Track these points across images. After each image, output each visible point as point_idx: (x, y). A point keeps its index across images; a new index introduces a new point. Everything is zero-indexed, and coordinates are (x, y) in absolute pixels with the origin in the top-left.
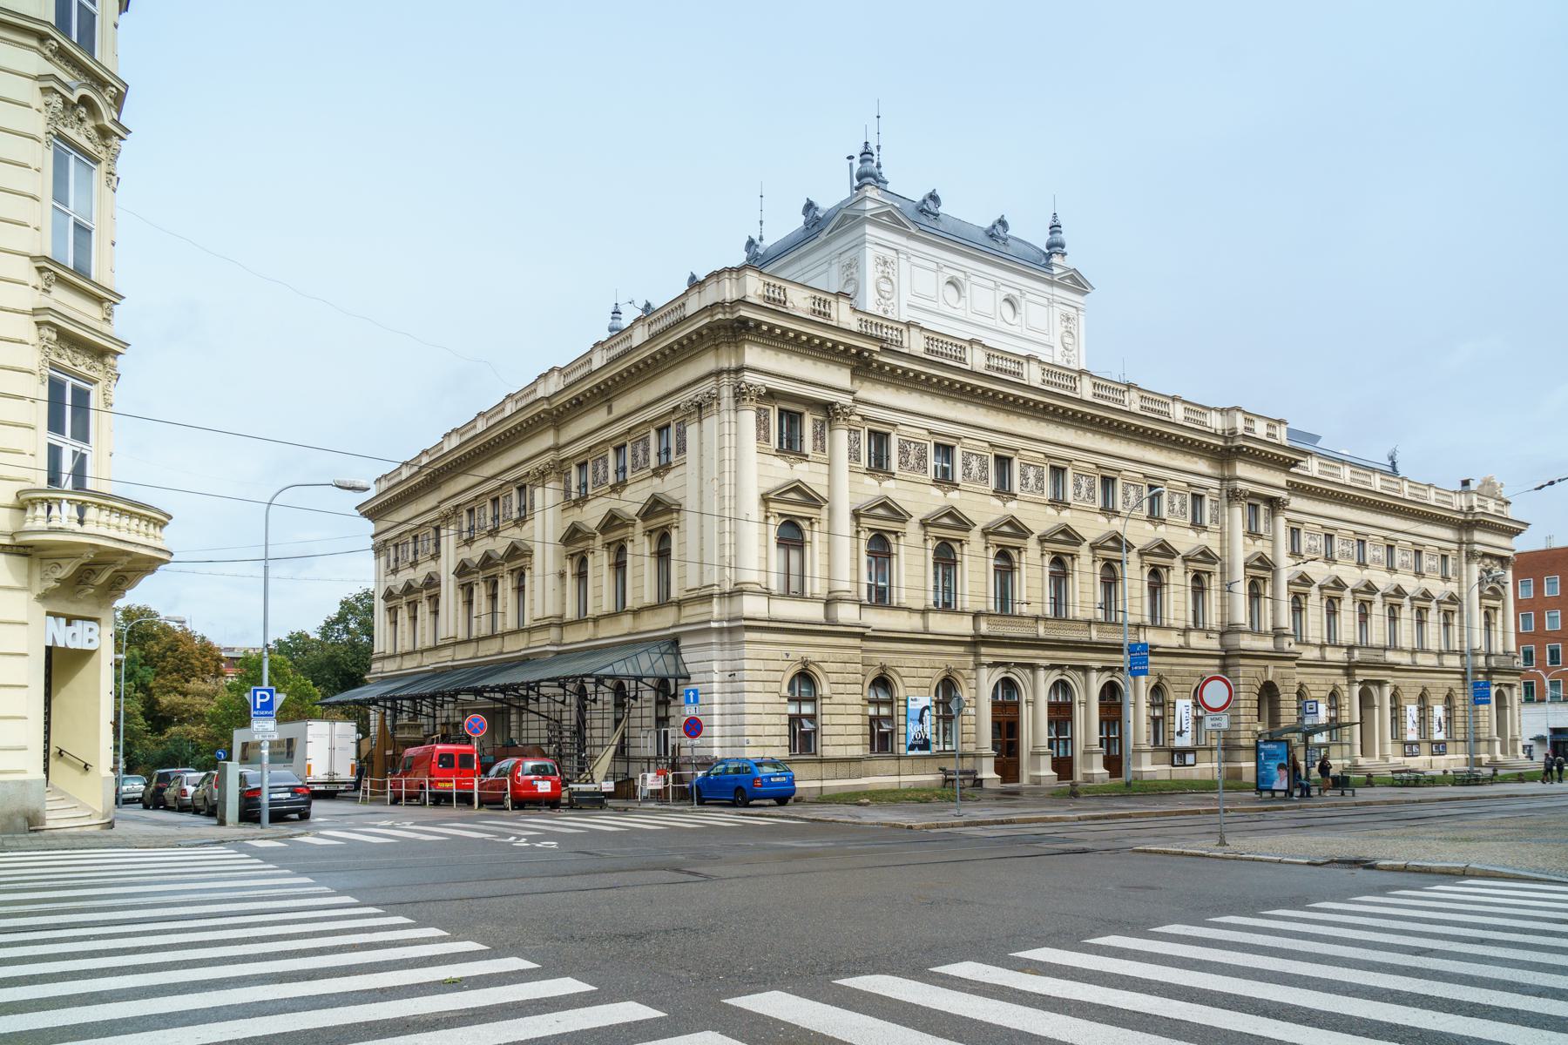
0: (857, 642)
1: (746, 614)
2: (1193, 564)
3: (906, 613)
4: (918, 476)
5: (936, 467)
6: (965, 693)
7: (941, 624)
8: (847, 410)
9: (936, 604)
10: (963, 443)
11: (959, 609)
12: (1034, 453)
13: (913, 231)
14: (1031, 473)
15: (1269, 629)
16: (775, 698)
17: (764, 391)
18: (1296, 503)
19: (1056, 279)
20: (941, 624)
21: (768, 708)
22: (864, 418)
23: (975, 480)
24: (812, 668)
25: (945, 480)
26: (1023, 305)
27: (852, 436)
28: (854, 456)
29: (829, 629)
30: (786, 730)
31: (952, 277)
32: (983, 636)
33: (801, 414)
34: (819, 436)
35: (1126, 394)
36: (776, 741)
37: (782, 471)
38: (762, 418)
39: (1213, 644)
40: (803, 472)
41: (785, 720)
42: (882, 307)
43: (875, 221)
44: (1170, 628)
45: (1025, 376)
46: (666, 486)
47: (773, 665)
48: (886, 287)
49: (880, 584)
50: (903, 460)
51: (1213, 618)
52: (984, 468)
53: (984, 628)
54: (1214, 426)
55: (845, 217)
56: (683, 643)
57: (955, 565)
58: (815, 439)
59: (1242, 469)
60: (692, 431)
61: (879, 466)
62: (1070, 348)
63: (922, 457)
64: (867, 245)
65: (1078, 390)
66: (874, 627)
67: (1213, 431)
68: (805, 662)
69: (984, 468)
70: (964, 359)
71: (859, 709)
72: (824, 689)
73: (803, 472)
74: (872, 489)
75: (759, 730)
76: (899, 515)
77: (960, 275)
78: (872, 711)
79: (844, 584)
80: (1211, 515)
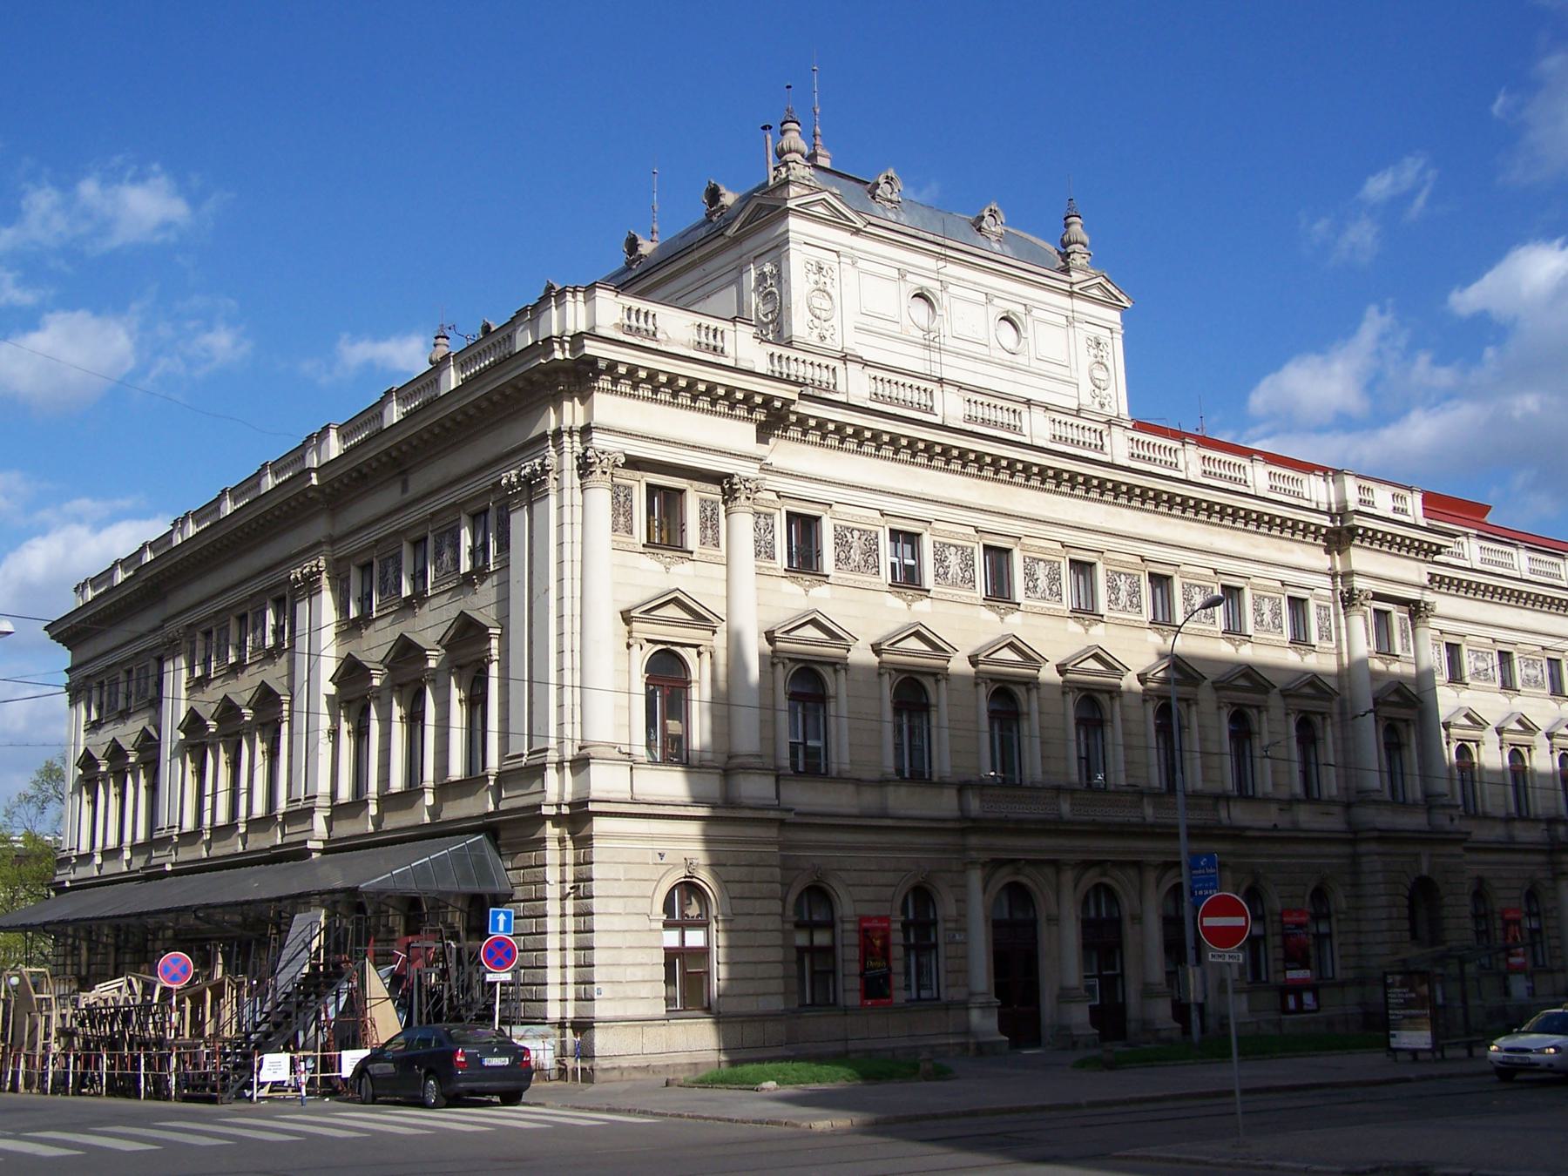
0: (772, 833)
1: (594, 795)
2: (1296, 701)
3: (851, 788)
4: (867, 579)
5: (893, 565)
6: (946, 907)
7: (905, 801)
8: (752, 486)
9: (900, 771)
10: (934, 529)
11: (935, 779)
12: (1045, 542)
13: (860, 225)
14: (1041, 572)
15: (1419, 795)
16: (639, 923)
17: (623, 460)
18: (1444, 603)
19: (1076, 288)
20: (905, 801)
21: (630, 939)
23: (954, 584)
25: (908, 580)
26: (1027, 323)
27: (762, 522)
28: (764, 550)
30: (661, 972)
31: (921, 288)
32: (974, 820)
33: (682, 492)
34: (709, 521)
35: (1180, 454)
36: (645, 991)
38: (622, 499)
39: (1334, 822)
40: (685, 576)
42: (816, 331)
44: (1267, 799)
45: (1026, 431)
46: (481, 604)
47: (637, 872)
49: (810, 743)
50: (842, 556)
51: (1330, 783)
52: (968, 564)
53: (975, 805)
54: (1314, 498)
55: (760, 207)
56: (504, 835)
57: (928, 712)
58: (703, 528)
59: (1361, 559)
60: (519, 521)
61: (805, 559)
62: (1103, 385)
63: (871, 551)
64: (791, 245)
65: (1107, 449)
66: (799, 808)
67: (1314, 506)
69: (968, 564)
70: (932, 408)
71: (777, 939)
73: (685, 576)
75: (617, 973)
77: (933, 286)
78: (801, 939)
80: (1320, 628)
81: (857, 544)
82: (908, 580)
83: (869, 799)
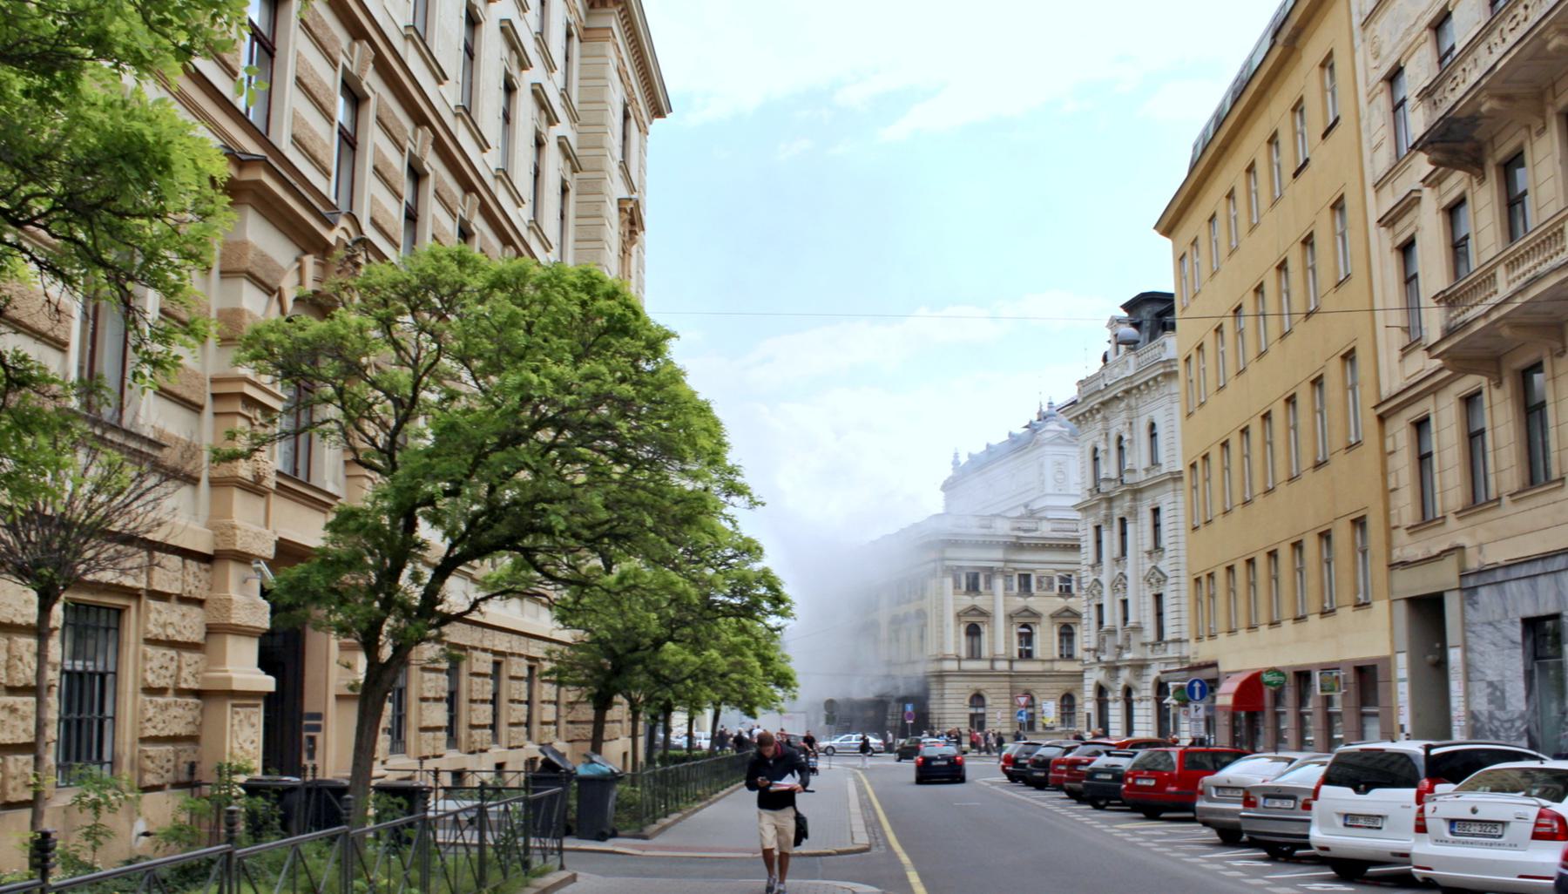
9: (1062, 656)
22: (1016, 569)
24: (982, 693)
25: (1066, 591)
28: (1008, 588)
29: (992, 674)
37: (967, 601)
40: (980, 601)
41: (967, 716)
43: (1052, 443)
48: (1059, 476)
63: (1051, 583)
68: (979, 690)
72: (988, 701)
74: (1020, 602)
76: (1036, 615)
79: (1001, 650)
81: (1044, 580)
82: (1066, 591)
83: (1047, 666)
